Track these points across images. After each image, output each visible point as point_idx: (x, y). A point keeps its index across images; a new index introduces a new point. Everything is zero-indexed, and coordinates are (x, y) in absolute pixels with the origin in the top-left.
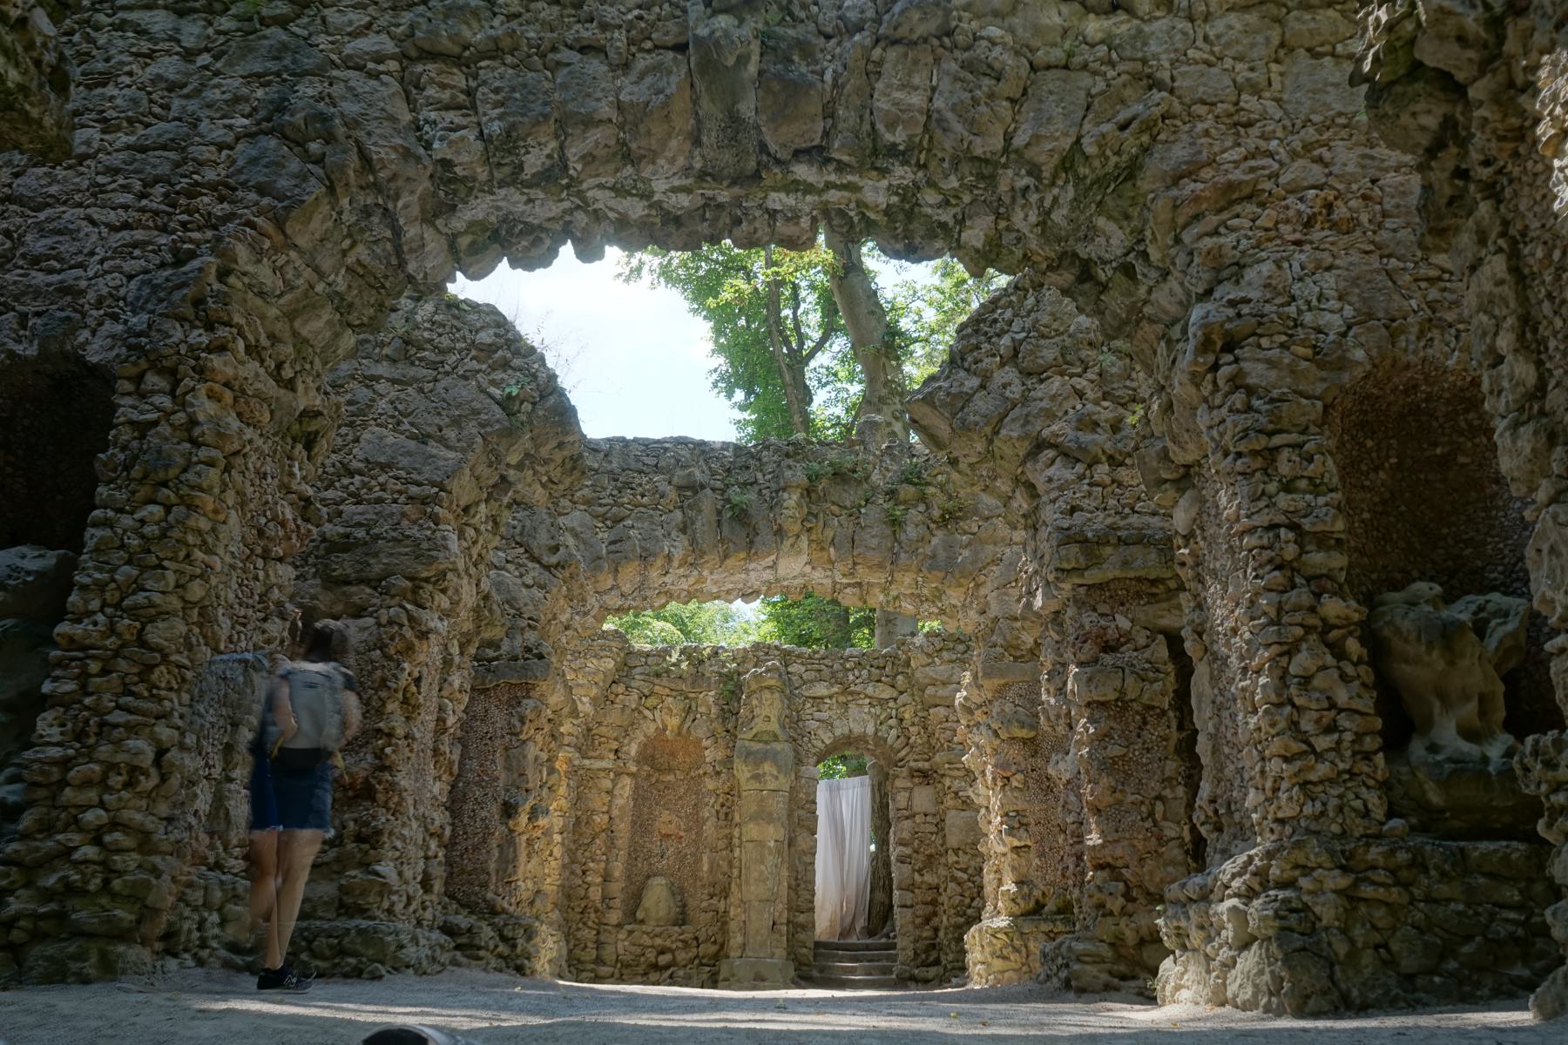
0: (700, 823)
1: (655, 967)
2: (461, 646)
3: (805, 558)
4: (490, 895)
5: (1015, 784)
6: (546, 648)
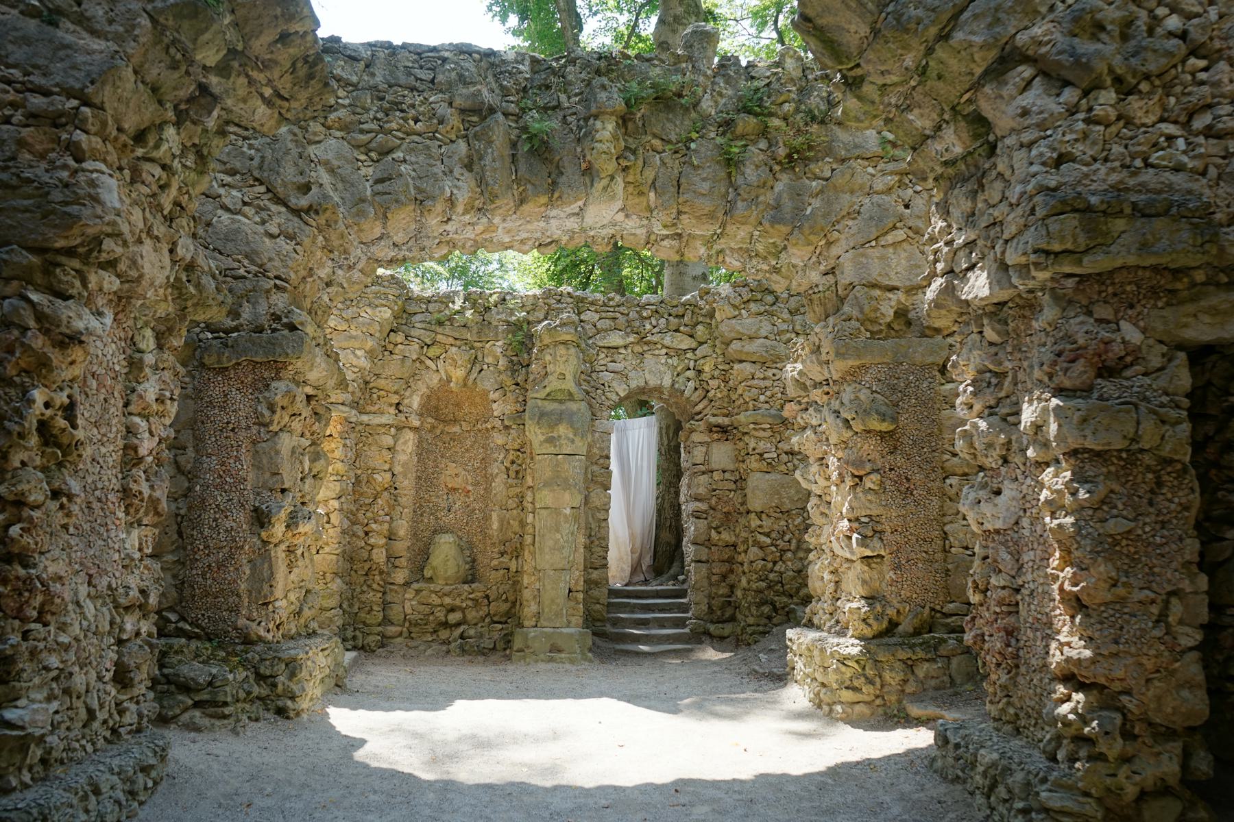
1: (445, 625)
2: (160, 337)
3: (619, 204)
4: (242, 622)
5: (869, 485)
6: (300, 316)
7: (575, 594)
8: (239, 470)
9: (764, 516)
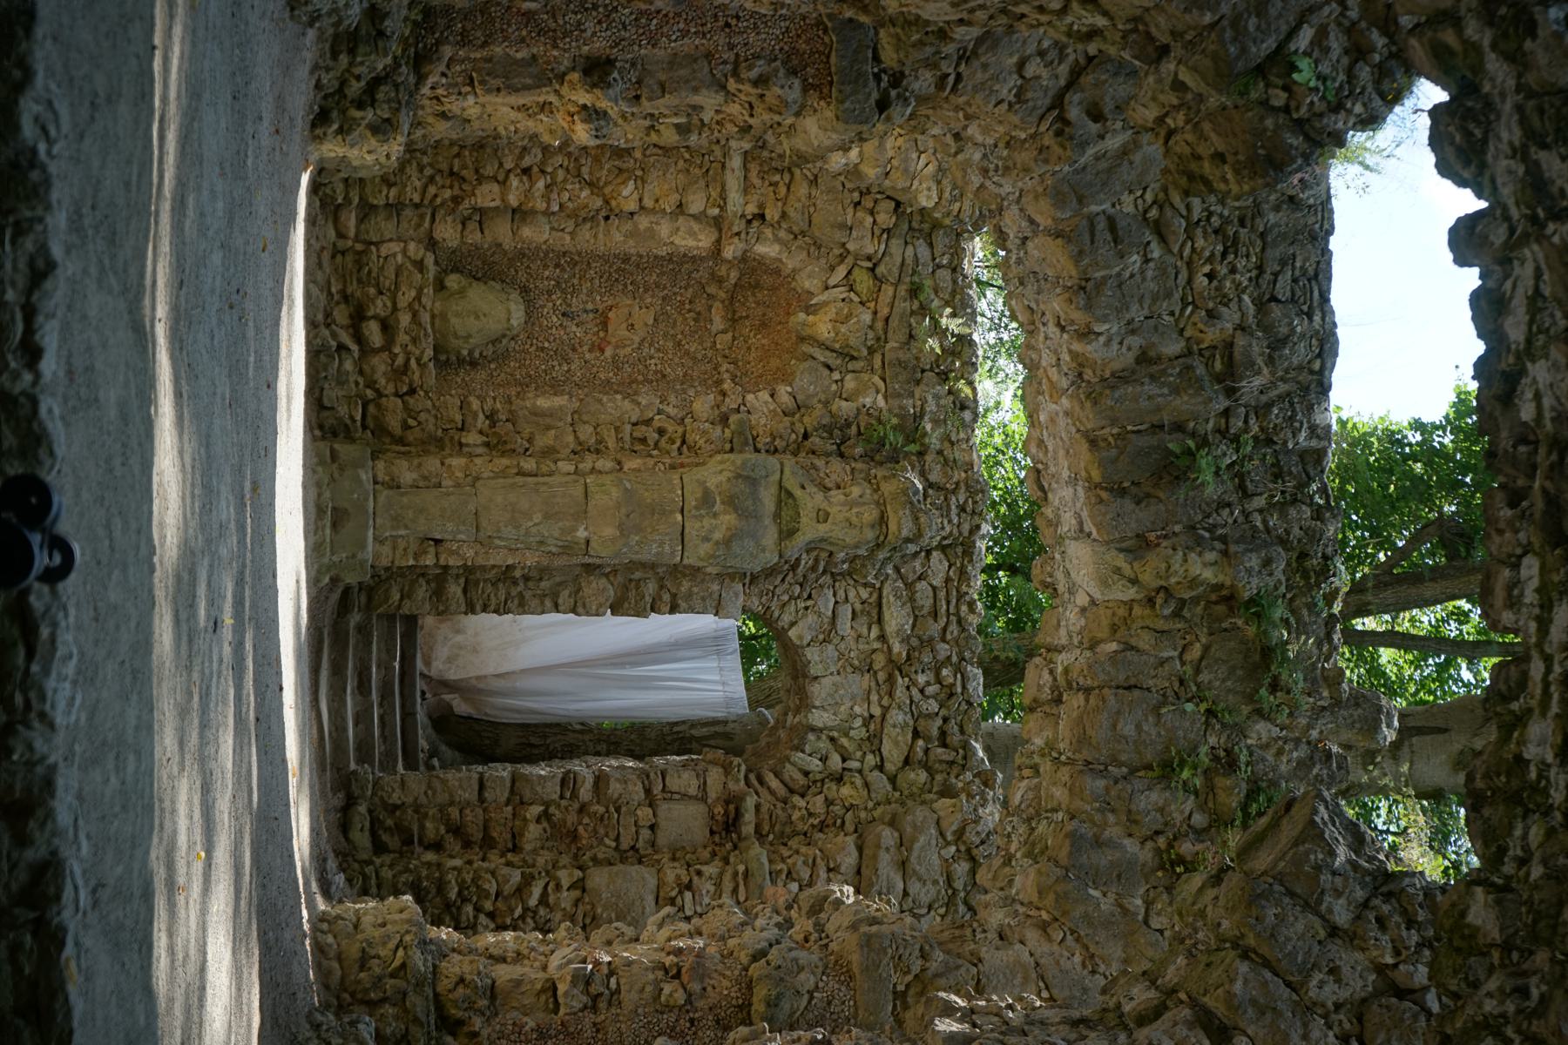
0: (628, 389)
1: (358, 317)
3: (1098, 596)
4: (447, 51)
5: (667, 988)
6: (899, 113)
7: (432, 550)
8: (668, 37)
9: (577, 893)
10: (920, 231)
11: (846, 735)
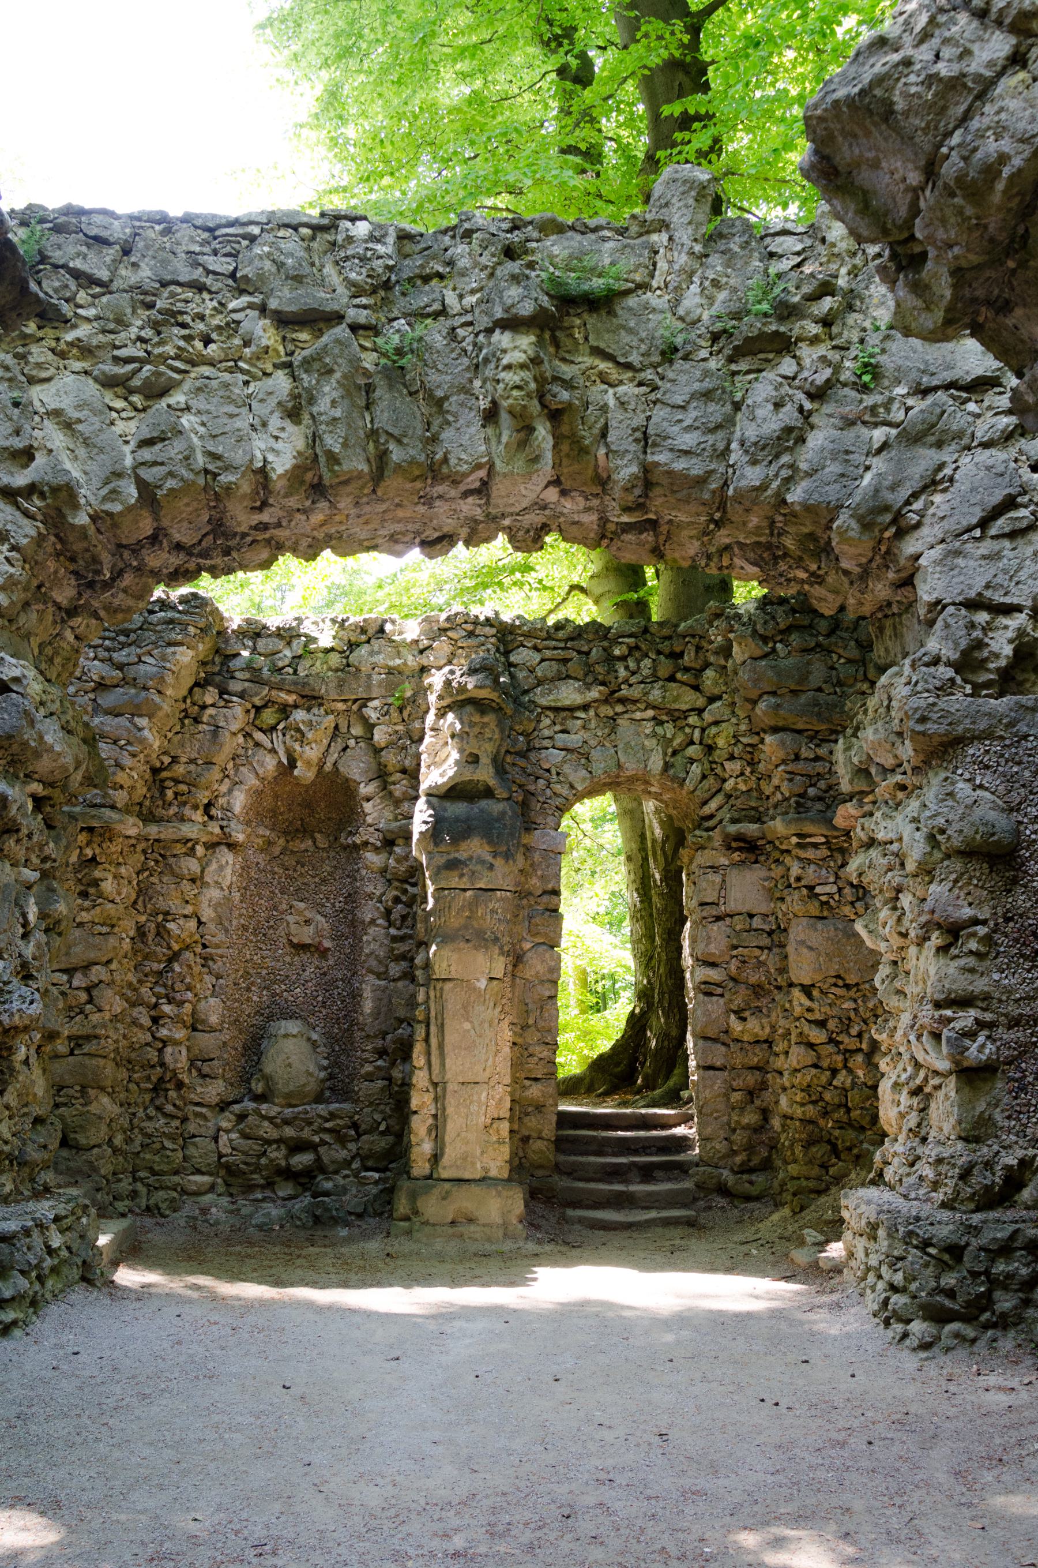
9: (815, 993)
10: (222, 664)
11: (671, 740)
